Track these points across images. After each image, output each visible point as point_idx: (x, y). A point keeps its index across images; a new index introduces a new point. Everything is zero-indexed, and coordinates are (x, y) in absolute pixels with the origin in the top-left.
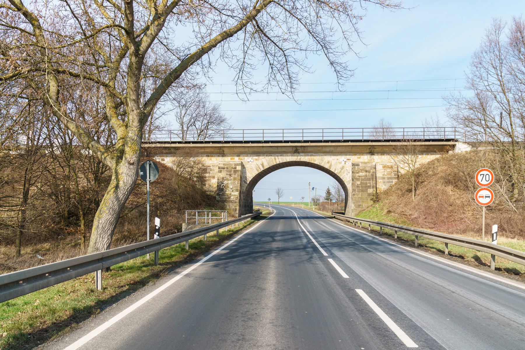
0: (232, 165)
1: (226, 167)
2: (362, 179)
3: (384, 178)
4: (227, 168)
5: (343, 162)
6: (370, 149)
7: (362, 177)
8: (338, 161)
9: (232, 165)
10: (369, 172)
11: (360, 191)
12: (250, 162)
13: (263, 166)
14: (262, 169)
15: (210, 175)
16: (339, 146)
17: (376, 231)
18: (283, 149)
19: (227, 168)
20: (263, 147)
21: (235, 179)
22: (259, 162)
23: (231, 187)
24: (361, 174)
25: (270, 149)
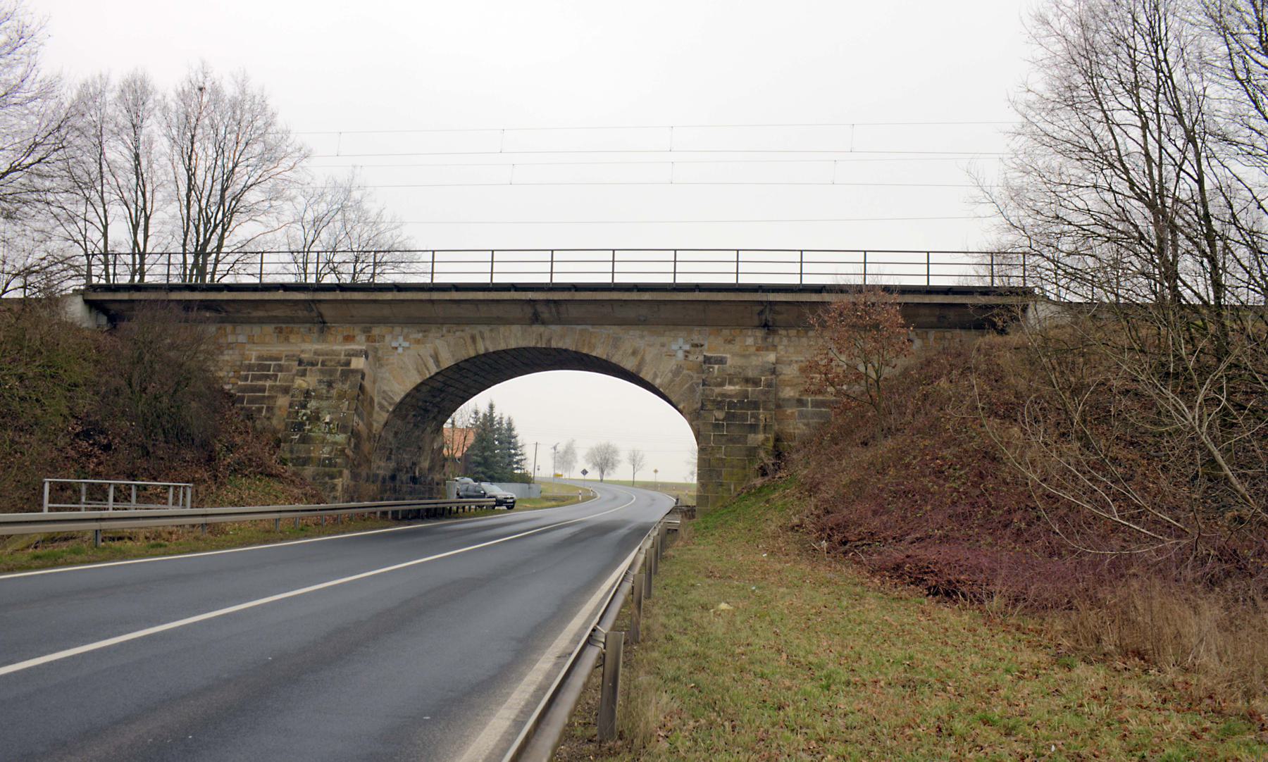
0: (339, 355)
1: (321, 358)
2: (729, 403)
3: (801, 402)
4: (323, 364)
5: (680, 355)
6: (761, 313)
7: (730, 396)
8: (665, 349)
9: (339, 355)
10: (756, 382)
11: (724, 440)
12: (400, 350)
13: (437, 361)
14: (434, 370)
15: (278, 383)
16: (498, 301)
17: (242, 323)
18: (496, 311)
19: (323, 364)
20: (432, 302)
21: (341, 396)
22: (426, 350)
23: (327, 420)
24: (729, 388)
25: (455, 311)
